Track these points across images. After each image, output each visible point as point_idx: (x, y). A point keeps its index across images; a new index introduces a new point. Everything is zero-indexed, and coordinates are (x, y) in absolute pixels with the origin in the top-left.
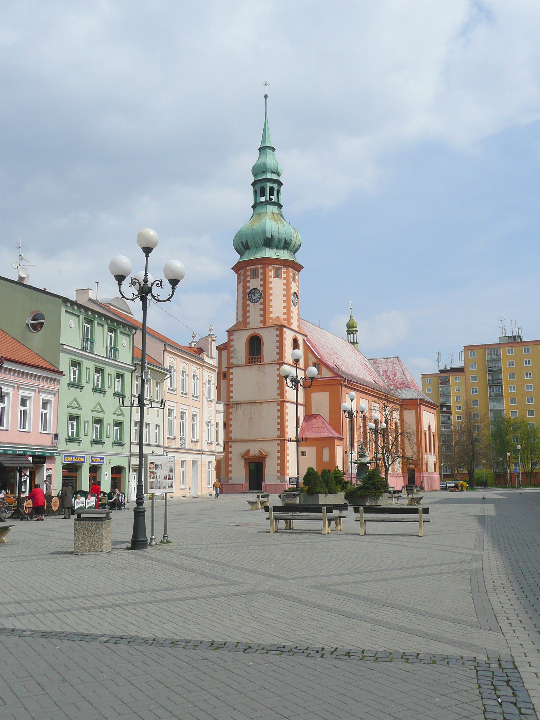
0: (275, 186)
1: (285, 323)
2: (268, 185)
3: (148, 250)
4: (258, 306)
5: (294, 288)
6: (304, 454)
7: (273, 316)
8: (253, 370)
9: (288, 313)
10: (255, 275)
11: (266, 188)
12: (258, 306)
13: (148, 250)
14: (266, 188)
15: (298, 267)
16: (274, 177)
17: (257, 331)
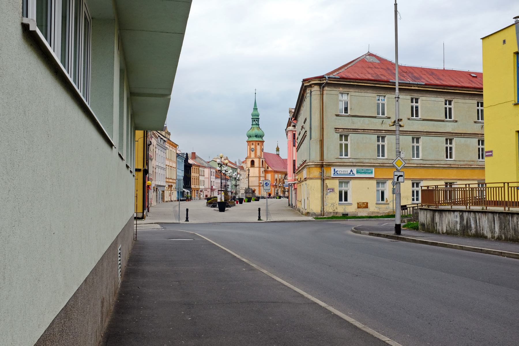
2: (256, 120)
4: (254, 152)
9: (261, 154)
10: (253, 144)
11: (256, 119)
12: (254, 152)
14: (256, 119)
16: (257, 117)
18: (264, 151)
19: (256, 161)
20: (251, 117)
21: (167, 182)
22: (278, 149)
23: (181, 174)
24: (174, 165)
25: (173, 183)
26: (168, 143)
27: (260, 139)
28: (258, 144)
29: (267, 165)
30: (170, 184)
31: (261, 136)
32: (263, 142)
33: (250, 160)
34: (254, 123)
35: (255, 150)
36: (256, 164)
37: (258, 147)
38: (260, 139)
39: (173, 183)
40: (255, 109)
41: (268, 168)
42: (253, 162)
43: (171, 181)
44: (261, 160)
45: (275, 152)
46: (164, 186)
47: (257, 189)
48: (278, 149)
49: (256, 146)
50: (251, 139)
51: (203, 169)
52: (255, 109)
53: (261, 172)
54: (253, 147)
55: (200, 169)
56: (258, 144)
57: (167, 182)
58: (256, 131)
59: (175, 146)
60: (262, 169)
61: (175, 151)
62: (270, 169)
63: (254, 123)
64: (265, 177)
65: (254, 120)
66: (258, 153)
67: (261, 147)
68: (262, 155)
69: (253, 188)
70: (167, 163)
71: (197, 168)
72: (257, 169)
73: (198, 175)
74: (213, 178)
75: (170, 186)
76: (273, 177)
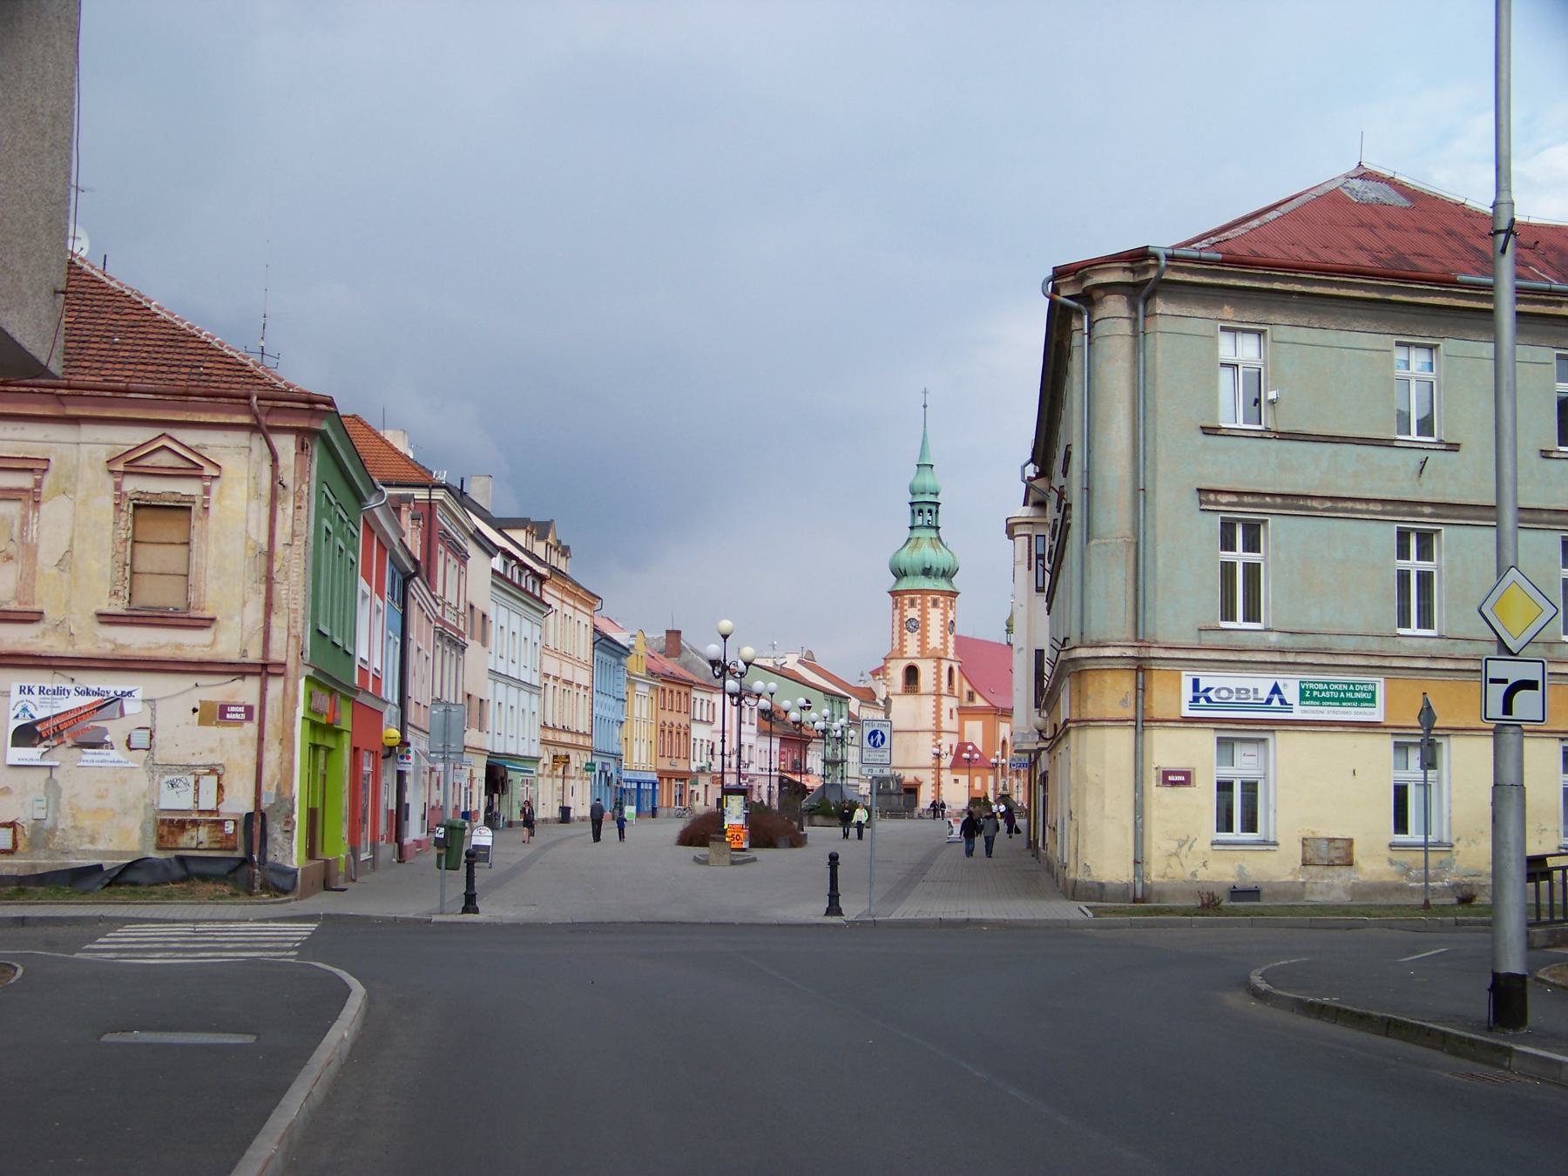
0: (934, 508)
1: (941, 654)
2: (926, 508)
3: (725, 637)
4: (916, 636)
5: (951, 616)
6: (956, 781)
7: (930, 646)
8: (910, 698)
10: (912, 604)
11: (925, 510)
12: (916, 636)
13: (725, 637)
14: (925, 510)
15: (954, 594)
16: (932, 498)
17: (917, 663)
18: (959, 630)
19: (926, 670)
20: (910, 498)
21: (544, 742)
24: (583, 677)
26: (555, 586)
27: (942, 585)
28: (935, 603)
29: (967, 687)
30: (562, 751)
32: (954, 594)
33: (904, 664)
34: (919, 521)
37: (935, 616)
41: (971, 697)
42: (912, 674)
43: (565, 738)
44: (945, 666)
45: (1001, 638)
46: (536, 760)
47: (927, 778)
49: (924, 611)
50: (905, 584)
51: (706, 697)
53: (945, 714)
54: (912, 613)
55: (695, 694)
56: (935, 603)
57: (544, 742)
58: (928, 554)
60: (949, 703)
61: (586, 620)
63: (919, 521)
64: (960, 732)
65: (917, 508)
66: (935, 640)
67: (945, 614)
68: (951, 645)
69: (909, 777)
71: (683, 690)
72: (929, 702)
73: (684, 720)
74: (750, 733)
75: (562, 761)
76: (989, 734)
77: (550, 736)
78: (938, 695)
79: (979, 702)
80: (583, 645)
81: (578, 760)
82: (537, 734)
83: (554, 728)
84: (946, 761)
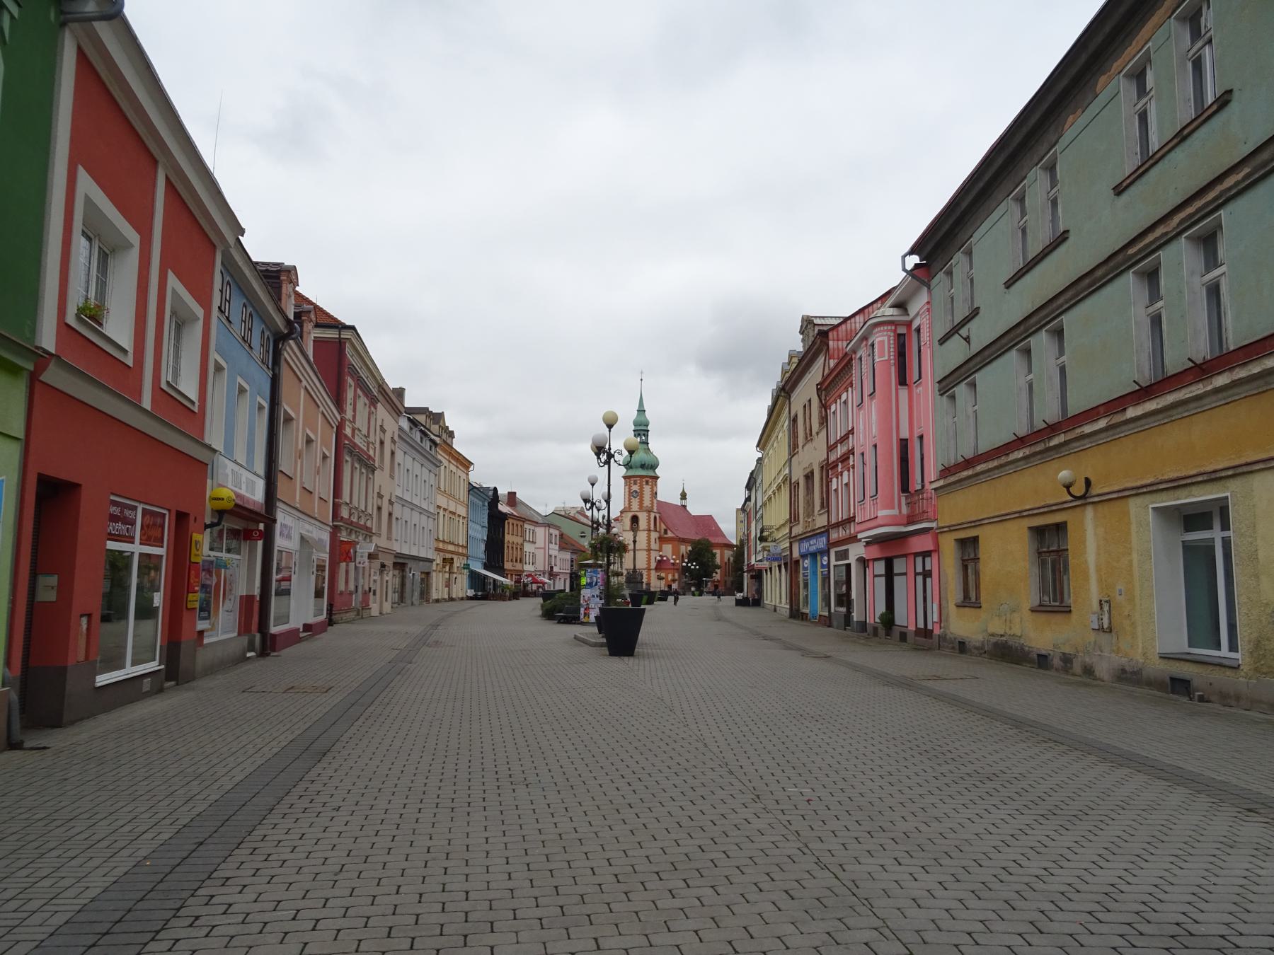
15: (657, 478)
19: (643, 517)
21: (437, 549)
22: (684, 496)
23: (480, 533)
24: (462, 511)
25: (458, 554)
27: (650, 473)
28: (647, 483)
29: (663, 527)
30: (448, 556)
31: (653, 467)
32: (657, 478)
33: (630, 515)
35: (640, 495)
36: (643, 523)
37: (647, 489)
38: (650, 473)
39: (458, 554)
40: (641, 411)
41: (666, 532)
42: (635, 520)
44: (652, 515)
45: (678, 502)
46: (431, 561)
48: (684, 496)
49: (641, 488)
50: (631, 473)
52: (641, 411)
54: (635, 488)
57: (437, 549)
59: (466, 464)
60: (654, 535)
62: (670, 534)
66: (647, 502)
70: (442, 501)
75: (448, 562)
77: (441, 546)
78: (649, 530)
79: (670, 534)
80: (462, 493)
81: (458, 562)
82: (433, 544)
83: (443, 541)
84: (653, 565)
